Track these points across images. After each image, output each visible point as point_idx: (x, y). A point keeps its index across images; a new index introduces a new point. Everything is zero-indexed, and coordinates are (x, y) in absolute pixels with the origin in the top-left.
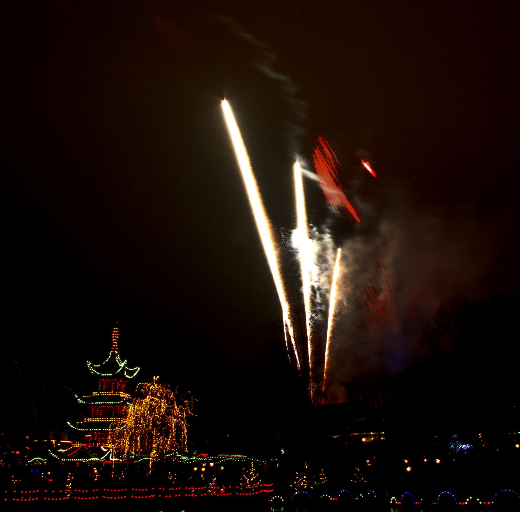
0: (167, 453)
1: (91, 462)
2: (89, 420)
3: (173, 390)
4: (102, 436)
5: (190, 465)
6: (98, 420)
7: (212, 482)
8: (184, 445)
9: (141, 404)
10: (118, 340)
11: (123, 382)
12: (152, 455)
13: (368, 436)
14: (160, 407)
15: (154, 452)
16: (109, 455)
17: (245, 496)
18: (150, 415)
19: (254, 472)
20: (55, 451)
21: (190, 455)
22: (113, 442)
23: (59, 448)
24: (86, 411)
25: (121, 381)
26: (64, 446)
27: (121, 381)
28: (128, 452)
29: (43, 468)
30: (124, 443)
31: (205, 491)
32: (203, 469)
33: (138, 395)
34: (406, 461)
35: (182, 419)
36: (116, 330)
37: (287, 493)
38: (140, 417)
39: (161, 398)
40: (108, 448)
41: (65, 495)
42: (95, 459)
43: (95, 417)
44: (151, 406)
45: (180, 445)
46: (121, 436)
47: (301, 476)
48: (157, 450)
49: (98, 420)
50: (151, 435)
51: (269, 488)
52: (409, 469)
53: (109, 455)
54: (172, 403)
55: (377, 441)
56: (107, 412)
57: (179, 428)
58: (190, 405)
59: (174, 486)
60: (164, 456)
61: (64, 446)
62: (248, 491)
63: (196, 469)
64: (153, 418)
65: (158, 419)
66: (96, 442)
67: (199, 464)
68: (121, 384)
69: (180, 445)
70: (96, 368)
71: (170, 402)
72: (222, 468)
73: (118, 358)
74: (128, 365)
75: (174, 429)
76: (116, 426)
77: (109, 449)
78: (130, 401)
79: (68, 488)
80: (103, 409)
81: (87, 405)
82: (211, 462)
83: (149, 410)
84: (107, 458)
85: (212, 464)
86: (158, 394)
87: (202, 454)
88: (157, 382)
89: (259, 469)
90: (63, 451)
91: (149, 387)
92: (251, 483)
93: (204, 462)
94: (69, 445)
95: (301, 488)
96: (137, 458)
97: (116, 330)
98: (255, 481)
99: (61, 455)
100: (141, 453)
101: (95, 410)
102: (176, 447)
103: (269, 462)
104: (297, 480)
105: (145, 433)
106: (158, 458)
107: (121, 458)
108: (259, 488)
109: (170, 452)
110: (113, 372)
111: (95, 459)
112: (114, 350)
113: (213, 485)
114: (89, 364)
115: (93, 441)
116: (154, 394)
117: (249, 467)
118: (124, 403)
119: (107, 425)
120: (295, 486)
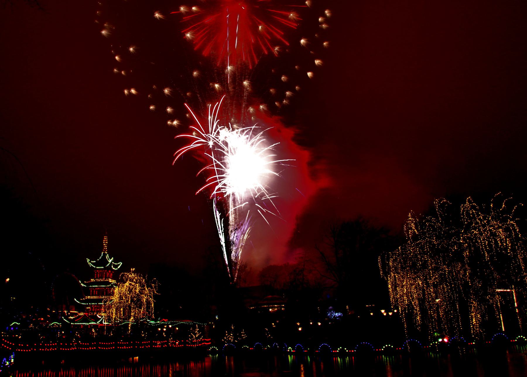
0: (141, 319)
3: (144, 278)
4: (98, 308)
6: (95, 297)
9: (123, 286)
10: (108, 245)
11: (111, 272)
12: (131, 320)
14: (136, 289)
15: (132, 318)
17: (192, 347)
18: (129, 294)
19: (198, 331)
21: (155, 320)
22: (105, 312)
24: (87, 291)
25: (110, 271)
26: (72, 315)
28: (115, 318)
29: (58, 329)
30: (112, 313)
31: (167, 343)
32: (165, 329)
33: (121, 281)
34: (298, 324)
35: (151, 297)
36: (105, 238)
37: (220, 344)
38: (122, 296)
39: (136, 283)
40: (102, 316)
42: (93, 323)
43: (93, 295)
44: (129, 288)
46: (110, 307)
47: (229, 334)
48: (134, 317)
49: (95, 297)
50: (130, 307)
51: (207, 342)
52: (300, 329)
54: (144, 286)
55: (279, 311)
56: (101, 292)
57: (148, 302)
58: (155, 287)
59: (145, 340)
62: (194, 343)
63: (160, 329)
64: (131, 297)
65: (134, 297)
67: (162, 326)
68: (110, 273)
70: (92, 263)
71: (142, 286)
73: (107, 256)
74: (114, 261)
75: (145, 303)
76: (107, 301)
78: (116, 285)
80: (99, 291)
83: (128, 290)
84: (101, 322)
88: (134, 272)
89: (201, 329)
90: (72, 318)
91: (128, 276)
92: (197, 338)
93: (165, 325)
94: (76, 314)
95: (229, 341)
96: (120, 322)
97: (105, 238)
98: (199, 337)
99: (71, 320)
100: (124, 319)
103: (208, 325)
104: (226, 336)
105: (126, 306)
107: (111, 322)
108: (201, 342)
109: (143, 318)
110: (104, 266)
111: (93, 323)
112: (105, 251)
114: (88, 260)
116: (131, 280)
117: (195, 328)
118: (112, 285)
119: (101, 301)
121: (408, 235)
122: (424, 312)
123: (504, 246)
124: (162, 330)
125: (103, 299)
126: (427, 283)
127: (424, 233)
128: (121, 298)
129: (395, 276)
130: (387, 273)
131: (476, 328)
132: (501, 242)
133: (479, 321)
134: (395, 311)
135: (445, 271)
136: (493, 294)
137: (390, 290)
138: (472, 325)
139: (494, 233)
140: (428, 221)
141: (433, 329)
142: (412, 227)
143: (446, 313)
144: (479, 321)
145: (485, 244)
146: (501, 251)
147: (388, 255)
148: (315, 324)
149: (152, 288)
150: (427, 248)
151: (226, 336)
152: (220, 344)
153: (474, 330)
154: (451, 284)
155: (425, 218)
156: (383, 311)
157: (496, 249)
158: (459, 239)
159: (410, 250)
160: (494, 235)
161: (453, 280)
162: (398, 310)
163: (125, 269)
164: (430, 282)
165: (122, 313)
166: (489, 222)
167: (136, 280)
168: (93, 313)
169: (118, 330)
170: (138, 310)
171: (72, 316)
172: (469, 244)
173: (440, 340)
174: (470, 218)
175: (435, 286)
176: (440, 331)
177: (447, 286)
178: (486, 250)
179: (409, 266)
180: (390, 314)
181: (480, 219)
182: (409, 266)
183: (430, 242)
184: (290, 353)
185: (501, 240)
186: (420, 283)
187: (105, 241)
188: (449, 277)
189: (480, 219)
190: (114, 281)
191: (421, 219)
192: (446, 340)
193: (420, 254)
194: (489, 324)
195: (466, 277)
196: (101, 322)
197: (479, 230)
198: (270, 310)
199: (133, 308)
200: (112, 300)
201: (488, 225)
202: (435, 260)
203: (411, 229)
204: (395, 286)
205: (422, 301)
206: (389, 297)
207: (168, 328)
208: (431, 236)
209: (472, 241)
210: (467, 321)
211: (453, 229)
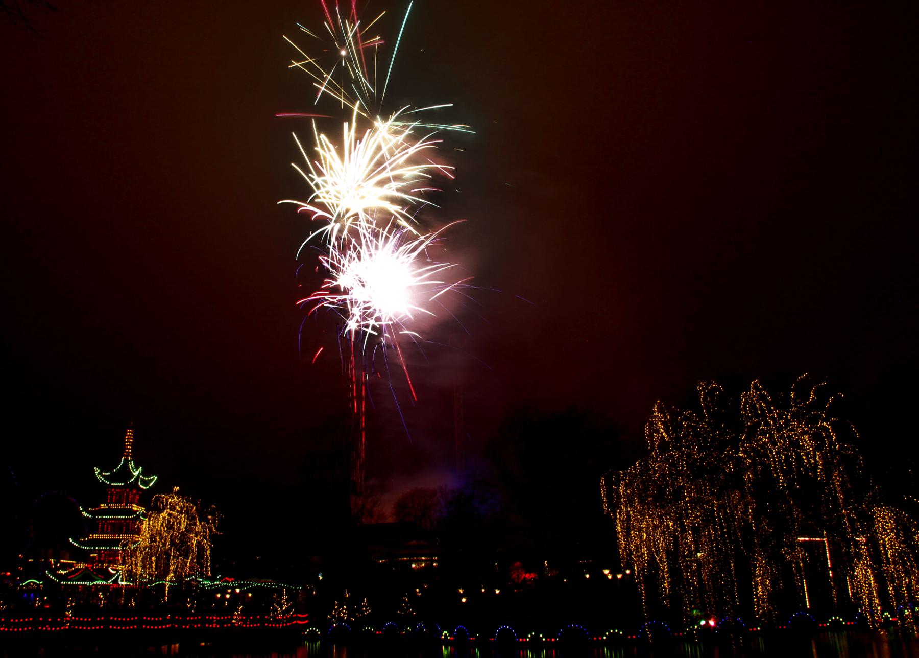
0: (186, 576)
1: (97, 585)
2: (95, 536)
3: (195, 504)
4: (110, 556)
5: (213, 590)
6: (107, 537)
7: (238, 611)
8: (207, 568)
10: (132, 445)
11: (137, 493)
12: (168, 578)
13: (418, 562)
16: (118, 578)
18: (166, 532)
19: (286, 600)
20: (53, 572)
21: (213, 579)
22: (124, 563)
23: (59, 569)
24: (93, 525)
25: (134, 492)
26: (64, 566)
27: (134, 492)
29: (37, 591)
30: (136, 565)
32: (228, 596)
33: (154, 508)
34: (461, 591)
35: (205, 538)
36: (129, 432)
37: (324, 625)
38: (155, 535)
39: (180, 512)
40: (117, 571)
41: (64, 624)
43: (102, 533)
44: (169, 521)
45: (202, 567)
47: (341, 606)
48: (175, 573)
49: (107, 537)
50: (168, 555)
51: (303, 619)
52: (464, 600)
53: (118, 578)
54: (194, 518)
55: (429, 567)
56: (117, 528)
58: (214, 520)
59: (194, 615)
60: (182, 579)
61: (64, 566)
62: (278, 621)
63: (219, 595)
65: (176, 537)
66: (102, 563)
67: (223, 590)
68: (135, 495)
69: (202, 567)
70: (104, 476)
71: (191, 518)
72: (250, 595)
74: (144, 473)
75: (195, 549)
77: (118, 571)
78: (145, 516)
79: (68, 616)
81: (94, 519)
82: (237, 587)
84: (116, 581)
85: (238, 590)
86: (178, 508)
87: (227, 579)
88: (177, 493)
89: (292, 596)
90: (63, 572)
91: (167, 500)
92: (283, 612)
94: (71, 565)
96: (151, 582)
97: (129, 432)
98: (288, 610)
101: (103, 525)
102: (197, 570)
103: (304, 589)
104: (336, 610)
106: (174, 582)
108: (291, 619)
109: (190, 575)
110: (125, 482)
113: (238, 615)
114: (97, 471)
115: (99, 561)
117: (280, 595)
118: (138, 516)
119: (116, 542)
120: (333, 616)
121: (652, 442)
122: (675, 572)
123: (810, 465)
124: (223, 596)
125: (120, 540)
126: (682, 525)
127: (678, 440)
128: (152, 538)
129: (628, 512)
130: (614, 506)
131: (763, 603)
132: (808, 458)
133: (768, 590)
134: (628, 572)
135: (713, 505)
136: (793, 545)
137: (620, 536)
138: (757, 597)
139: (796, 439)
140: (686, 419)
141: (691, 603)
142: (659, 429)
143: (714, 577)
144: (768, 590)
145: (780, 461)
146: (807, 472)
147: (618, 475)
148: (491, 591)
149: (208, 522)
150: (682, 466)
151: (336, 610)
152: (324, 625)
153: (758, 605)
154: (722, 528)
155: (680, 414)
156: (606, 572)
157: (798, 469)
158: (738, 451)
159: (654, 468)
160: (795, 444)
161: (726, 520)
162: (632, 570)
163: (163, 487)
164: (686, 522)
165: (154, 565)
166: (787, 423)
167: (182, 508)
168: (102, 565)
169: (146, 596)
170: (183, 561)
171: (62, 570)
172: (753, 460)
173: (703, 623)
174: (756, 415)
175: (696, 531)
176: (702, 608)
177: (715, 530)
178: (782, 470)
179: (653, 495)
180: (619, 576)
181: (772, 418)
182: (653, 495)
183: (689, 455)
184: (446, 642)
185: (807, 454)
186: (671, 524)
187: (129, 437)
188: (719, 516)
189: (772, 418)
190: (141, 510)
191: (674, 415)
192: (712, 623)
193: (671, 475)
194: (784, 596)
195: (748, 516)
196: (116, 581)
197: (771, 436)
198: (413, 565)
199: (174, 557)
200: (136, 542)
201: (786, 428)
202: (696, 486)
203: (657, 431)
204: (627, 529)
205: (673, 555)
206: (616, 546)
207: (233, 593)
208: (690, 445)
209: (760, 454)
210: (747, 591)
211: (728, 434)
